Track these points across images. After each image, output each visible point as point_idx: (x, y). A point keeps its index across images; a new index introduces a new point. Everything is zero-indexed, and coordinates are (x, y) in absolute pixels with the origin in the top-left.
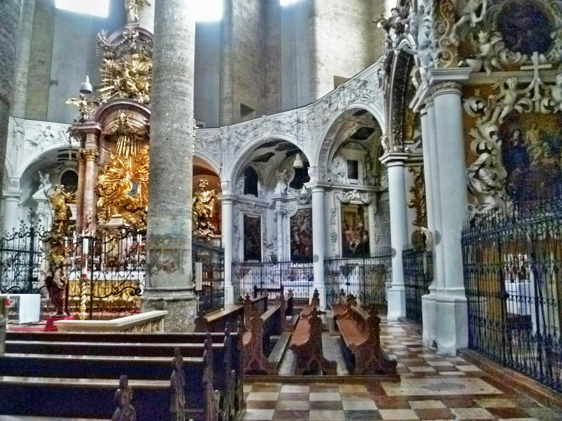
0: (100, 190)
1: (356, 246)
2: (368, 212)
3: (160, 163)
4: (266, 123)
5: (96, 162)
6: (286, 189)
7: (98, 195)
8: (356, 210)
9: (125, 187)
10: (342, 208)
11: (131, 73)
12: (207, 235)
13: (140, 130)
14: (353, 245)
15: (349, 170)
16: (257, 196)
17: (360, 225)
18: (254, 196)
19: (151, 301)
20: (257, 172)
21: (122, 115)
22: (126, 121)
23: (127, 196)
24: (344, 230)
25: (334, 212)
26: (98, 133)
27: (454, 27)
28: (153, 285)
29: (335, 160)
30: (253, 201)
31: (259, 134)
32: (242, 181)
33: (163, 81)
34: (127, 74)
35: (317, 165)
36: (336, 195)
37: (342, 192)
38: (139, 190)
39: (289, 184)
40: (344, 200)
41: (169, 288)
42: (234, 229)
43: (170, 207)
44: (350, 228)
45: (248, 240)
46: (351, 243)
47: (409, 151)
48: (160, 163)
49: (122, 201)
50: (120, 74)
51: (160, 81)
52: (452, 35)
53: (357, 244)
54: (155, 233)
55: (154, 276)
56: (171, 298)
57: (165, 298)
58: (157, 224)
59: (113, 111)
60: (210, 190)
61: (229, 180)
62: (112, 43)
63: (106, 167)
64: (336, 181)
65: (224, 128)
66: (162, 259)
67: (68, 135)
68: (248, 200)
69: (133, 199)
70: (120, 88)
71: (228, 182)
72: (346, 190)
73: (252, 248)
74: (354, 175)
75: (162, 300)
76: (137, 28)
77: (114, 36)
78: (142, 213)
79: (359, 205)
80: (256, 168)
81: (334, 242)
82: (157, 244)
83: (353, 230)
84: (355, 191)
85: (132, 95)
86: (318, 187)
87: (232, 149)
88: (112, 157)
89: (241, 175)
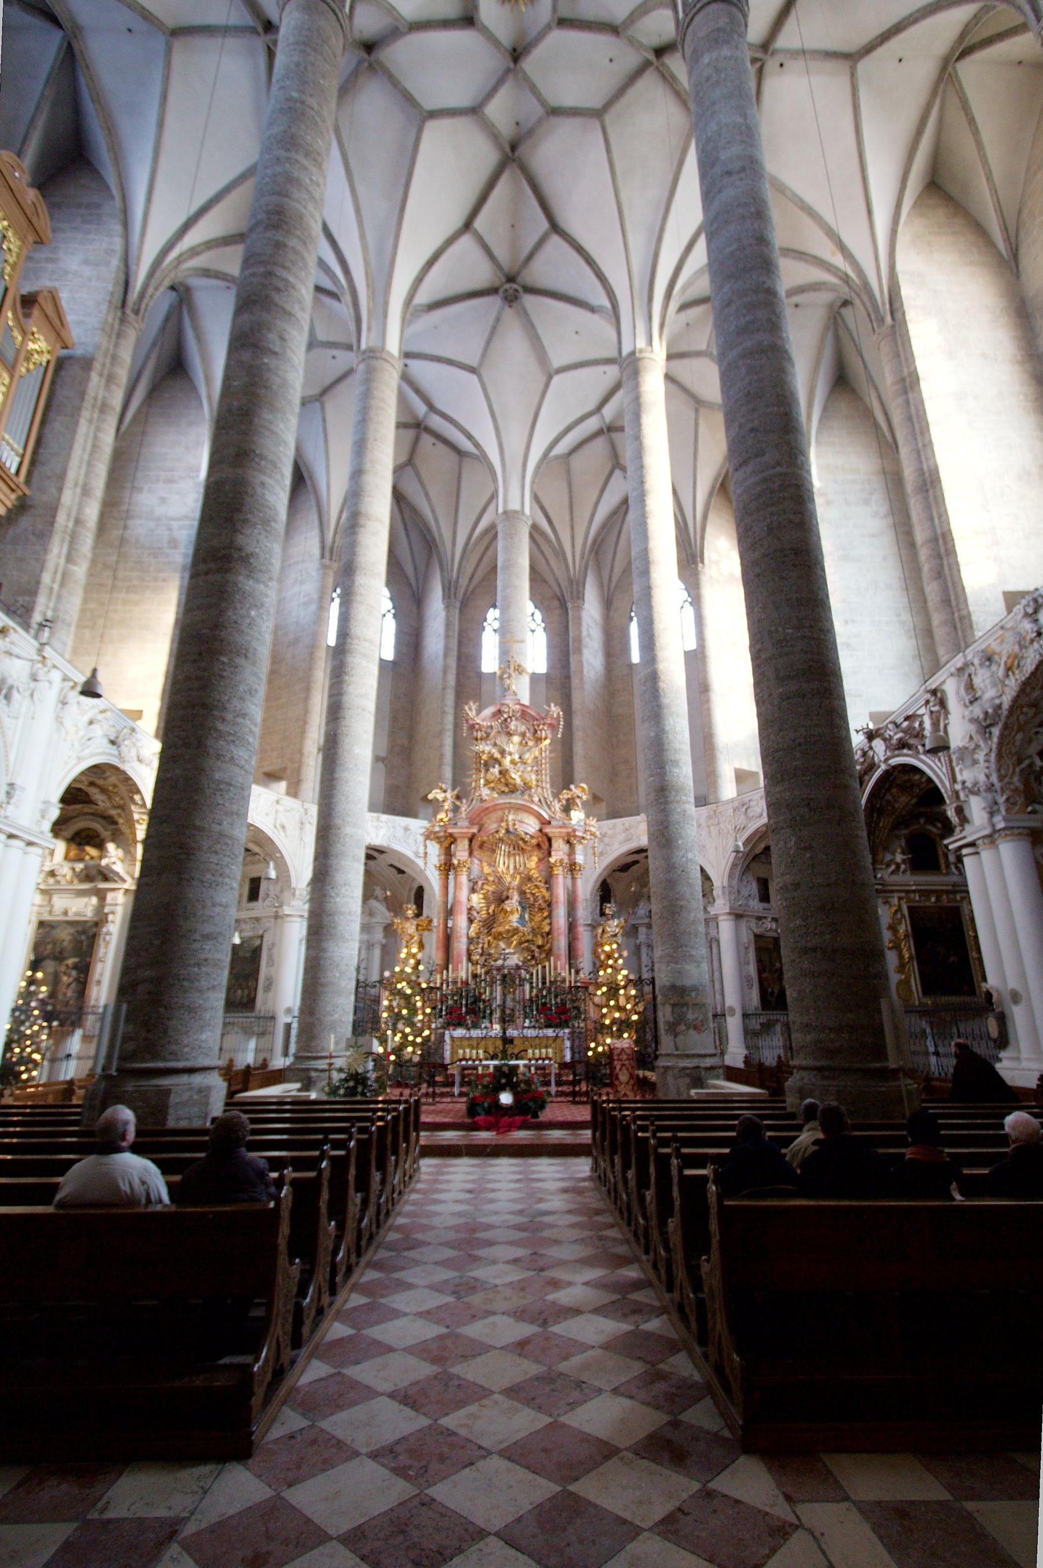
3: (677, 899)
5: (469, 876)
7: (471, 921)
8: (771, 946)
9: (512, 912)
10: (756, 942)
11: (513, 762)
13: (532, 837)
14: (773, 993)
19: (685, 1068)
22: (514, 825)
23: (515, 924)
25: (747, 948)
27: (1018, 770)
28: (680, 1046)
33: (672, 802)
34: (507, 761)
37: (754, 921)
38: (527, 916)
40: (757, 931)
41: (703, 1052)
43: (694, 952)
47: (881, 878)
48: (677, 899)
49: (508, 931)
52: (1016, 779)
53: (776, 991)
54: (678, 984)
55: (681, 1037)
56: (708, 1065)
57: (702, 1065)
58: (679, 972)
59: (495, 810)
60: (619, 918)
63: (480, 883)
64: (747, 905)
66: (690, 1016)
67: (421, 839)
69: (521, 928)
70: (499, 779)
72: (759, 918)
74: (765, 897)
75: (698, 1067)
77: (488, 711)
78: (533, 948)
82: (682, 997)
85: (513, 790)
88: (487, 870)
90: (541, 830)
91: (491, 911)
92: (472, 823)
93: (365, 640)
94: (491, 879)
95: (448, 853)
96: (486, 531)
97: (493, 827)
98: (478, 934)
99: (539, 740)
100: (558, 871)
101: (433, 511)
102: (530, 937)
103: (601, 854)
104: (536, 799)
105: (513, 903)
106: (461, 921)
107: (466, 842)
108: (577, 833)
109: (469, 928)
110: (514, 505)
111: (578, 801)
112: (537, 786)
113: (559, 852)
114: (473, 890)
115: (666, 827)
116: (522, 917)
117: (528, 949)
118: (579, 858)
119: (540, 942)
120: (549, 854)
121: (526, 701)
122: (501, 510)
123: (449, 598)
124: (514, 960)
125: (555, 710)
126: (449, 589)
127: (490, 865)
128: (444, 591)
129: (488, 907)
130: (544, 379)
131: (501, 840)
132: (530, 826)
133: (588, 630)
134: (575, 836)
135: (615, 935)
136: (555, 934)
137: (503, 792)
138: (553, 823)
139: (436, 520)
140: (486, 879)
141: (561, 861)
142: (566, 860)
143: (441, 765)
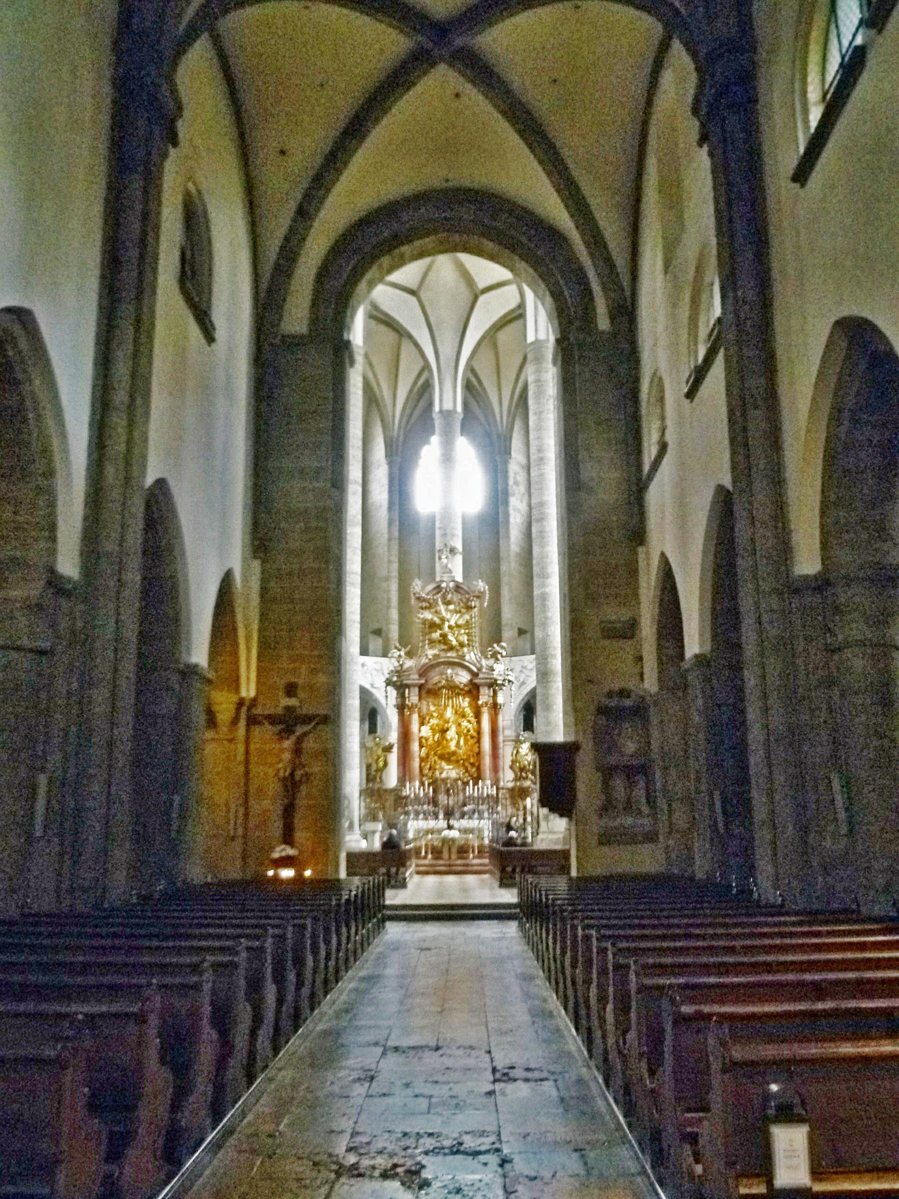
0: (424, 741)
9: (451, 740)
11: (450, 627)
13: (465, 685)
21: (449, 671)
26: (421, 687)
49: (448, 753)
50: (440, 627)
51: (548, 682)
62: (428, 594)
67: (384, 684)
76: (454, 581)
77: (430, 587)
78: (467, 764)
85: (451, 648)
88: (432, 708)
90: (471, 681)
91: (436, 739)
92: (421, 675)
93: (353, 573)
94: (435, 715)
95: (402, 696)
96: (423, 385)
97: (436, 679)
98: (428, 755)
99: (469, 608)
100: (485, 710)
101: (375, 375)
102: (465, 757)
103: (523, 683)
104: (467, 658)
105: (452, 734)
106: (415, 746)
107: (417, 689)
108: (499, 682)
109: (420, 751)
110: (448, 406)
111: (499, 656)
112: (469, 645)
113: (485, 697)
114: (422, 724)
115: (547, 698)
116: (458, 742)
117: (463, 765)
118: (500, 700)
119: (472, 760)
120: (478, 699)
121: (459, 578)
122: (437, 408)
123: (391, 455)
124: (453, 774)
125: (481, 585)
126: (391, 446)
127: (435, 705)
128: (386, 448)
129: (434, 736)
130: (472, 298)
131: (443, 687)
132: (463, 678)
133: (515, 478)
134: (497, 685)
135: (527, 755)
136: (482, 755)
137: (443, 650)
138: (481, 676)
139: (379, 385)
140: (432, 716)
141: (486, 704)
142: (491, 701)
143: (388, 607)
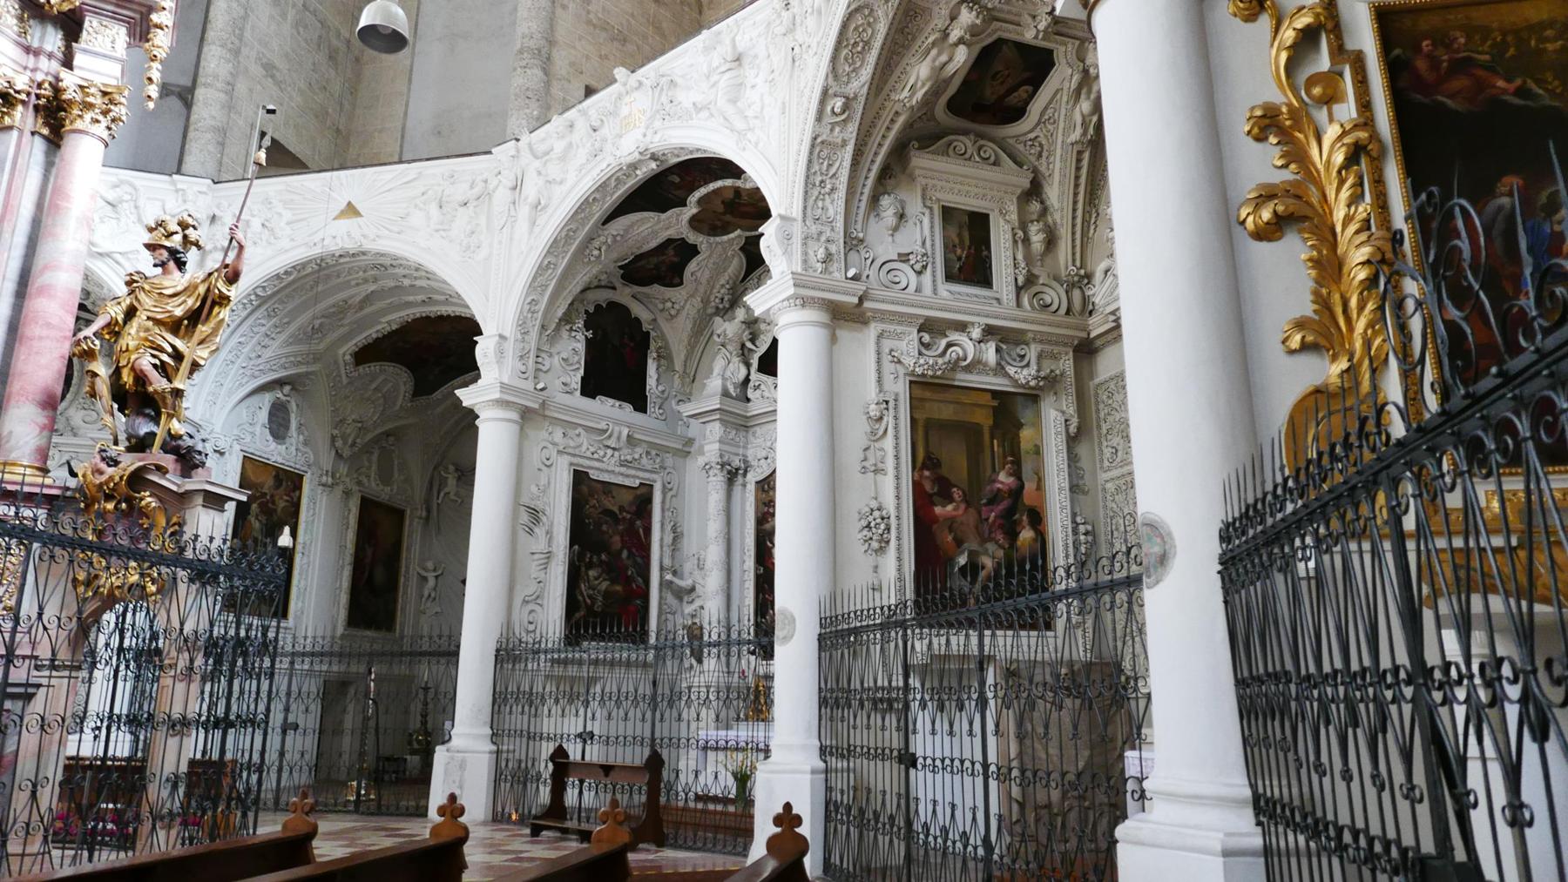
1: (983, 574)
2: (1037, 424)
4: (627, 99)
6: (747, 380)
10: (915, 403)
12: (137, 479)
14: (973, 568)
15: (948, 247)
16: (640, 405)
17: (1004, 479)
18: (628, 407)
20: (646, 327)
24: (923, 504)
29: (886, 201)
30: (618, 422)
31: (608, 147)
32: (574, 346)
35: (796, 212)
36: (887, 344)
39: (755, 362)
42: (525, 517)
44: (956, 493)
45: (590, 566)
46: (962, 560)
53: (988, 562)
61: (507, 334)
65: (502, 152)
68: (602, 418)
71: (502, 337)
73: (607, 594)
79: (995, 394)
80: (638, 310)
81: (881, 550)
83: (968, 501)
84: (976, 333)
86: (805, 302)
87: (524, 211)
89: (567, 319)
